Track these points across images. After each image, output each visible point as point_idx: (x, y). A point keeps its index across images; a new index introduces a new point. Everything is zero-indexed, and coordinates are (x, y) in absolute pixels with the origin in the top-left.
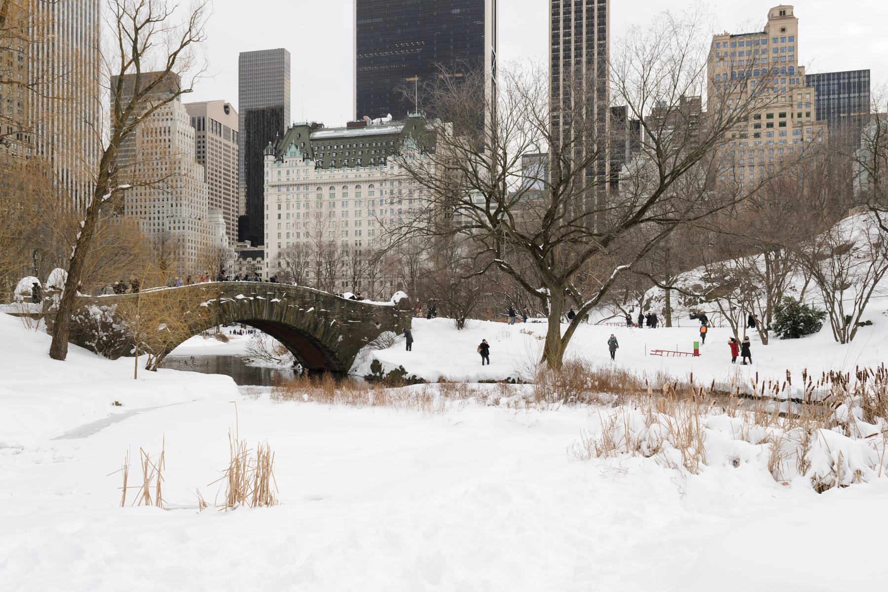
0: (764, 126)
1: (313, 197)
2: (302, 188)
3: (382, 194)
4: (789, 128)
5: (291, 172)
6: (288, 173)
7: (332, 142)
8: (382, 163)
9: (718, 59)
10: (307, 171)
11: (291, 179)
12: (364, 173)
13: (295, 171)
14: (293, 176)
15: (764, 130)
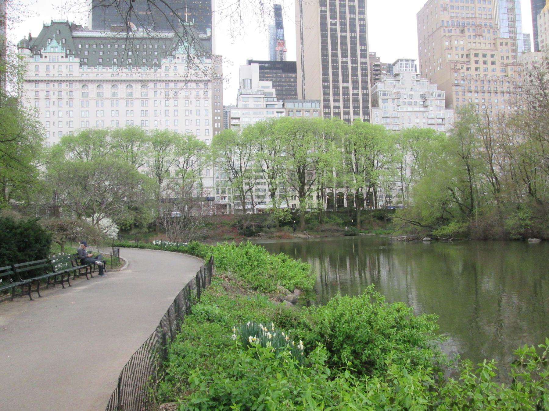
0: (481, 62)
1: (77, 94)
2: (64, 85)
3: (156, 95)
4: (497, 66)
5: (51, 67)
6: (48, 67)
7: (99, 41)
8: (155, 65)
9: (442, 9)
10: (72, 67)
11: (51, 75)
12: (136, 74)
13: (56, 67)
14: (54, 74)
15: (481, 65)
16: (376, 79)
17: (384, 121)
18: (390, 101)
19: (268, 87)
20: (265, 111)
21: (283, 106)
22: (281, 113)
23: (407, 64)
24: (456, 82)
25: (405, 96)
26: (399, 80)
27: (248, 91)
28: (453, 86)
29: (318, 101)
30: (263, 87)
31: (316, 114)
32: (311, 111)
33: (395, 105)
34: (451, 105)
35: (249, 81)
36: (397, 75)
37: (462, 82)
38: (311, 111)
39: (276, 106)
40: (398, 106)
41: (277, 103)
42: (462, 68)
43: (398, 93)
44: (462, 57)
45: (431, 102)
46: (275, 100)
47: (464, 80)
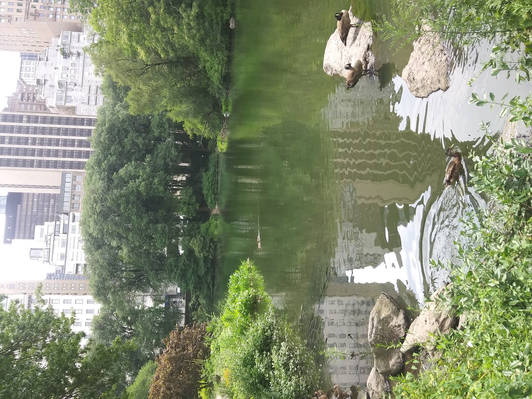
16: (42, 105)
17: (93, 102)
18: (69, 93)
19: (42, 230)
20: (71, 235)
21: (67, 214)
22: (74, 217)
23: (26, 69)
24: (51, 16)
25: (65, 76)
26: (45, 80)
27: (46, 253)
28: (55, 20)
29: (64, 175)
30: (41, 236)
31: (79, 178)
32: (74, 183)
33: (74, 88)
34: (79, 25)
35: (32, 251)
36: (38, 81)
37: (52, 9)
38: (74, 183)
39: (66, 222)
40: (76, 85)
41: (62, 222)
42: (35, 7)
43: (60, 84)
44: (21, 5)
45: (73, 48)
46: (58, 223)
47: (49, 7)
